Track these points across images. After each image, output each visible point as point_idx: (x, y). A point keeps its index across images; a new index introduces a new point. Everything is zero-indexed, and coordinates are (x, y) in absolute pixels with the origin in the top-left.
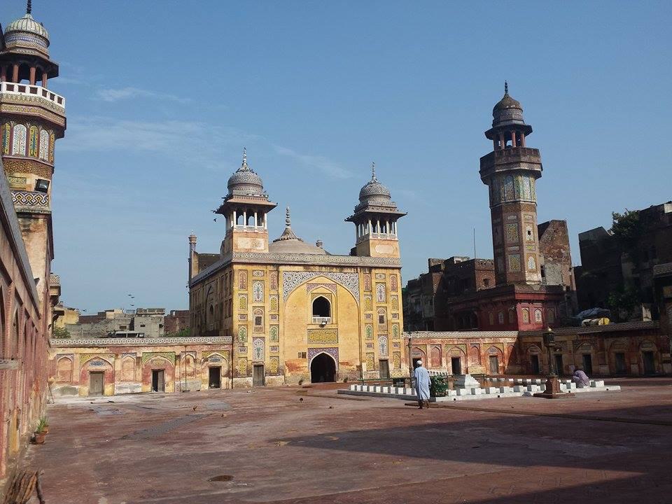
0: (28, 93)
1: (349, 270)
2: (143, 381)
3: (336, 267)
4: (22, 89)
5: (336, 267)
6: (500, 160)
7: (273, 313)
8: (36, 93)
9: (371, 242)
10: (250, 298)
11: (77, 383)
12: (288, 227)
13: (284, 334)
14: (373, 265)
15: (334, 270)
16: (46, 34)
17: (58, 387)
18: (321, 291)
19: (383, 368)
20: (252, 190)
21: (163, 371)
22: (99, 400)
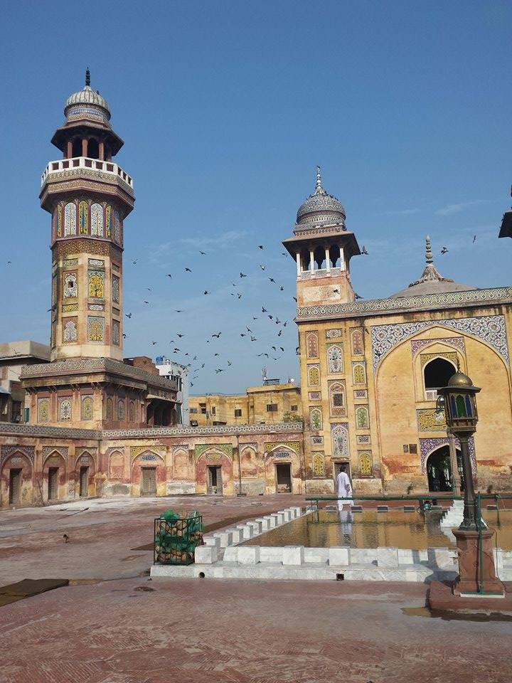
0: (71, 167)
1: (485, 313)
2: (197, 480)
3: (461, 309)
4: (66, 165)
5: (461, 309)
8: (78, 165)
10: (324, 368)
11: (129, 482)
13: (377, 418)
15: (458, 315)
16: (100, 100)
17: (110, 484)
18: (439, 350)
20: (322, 219)
21: (220, 467)
22: (149, 500)
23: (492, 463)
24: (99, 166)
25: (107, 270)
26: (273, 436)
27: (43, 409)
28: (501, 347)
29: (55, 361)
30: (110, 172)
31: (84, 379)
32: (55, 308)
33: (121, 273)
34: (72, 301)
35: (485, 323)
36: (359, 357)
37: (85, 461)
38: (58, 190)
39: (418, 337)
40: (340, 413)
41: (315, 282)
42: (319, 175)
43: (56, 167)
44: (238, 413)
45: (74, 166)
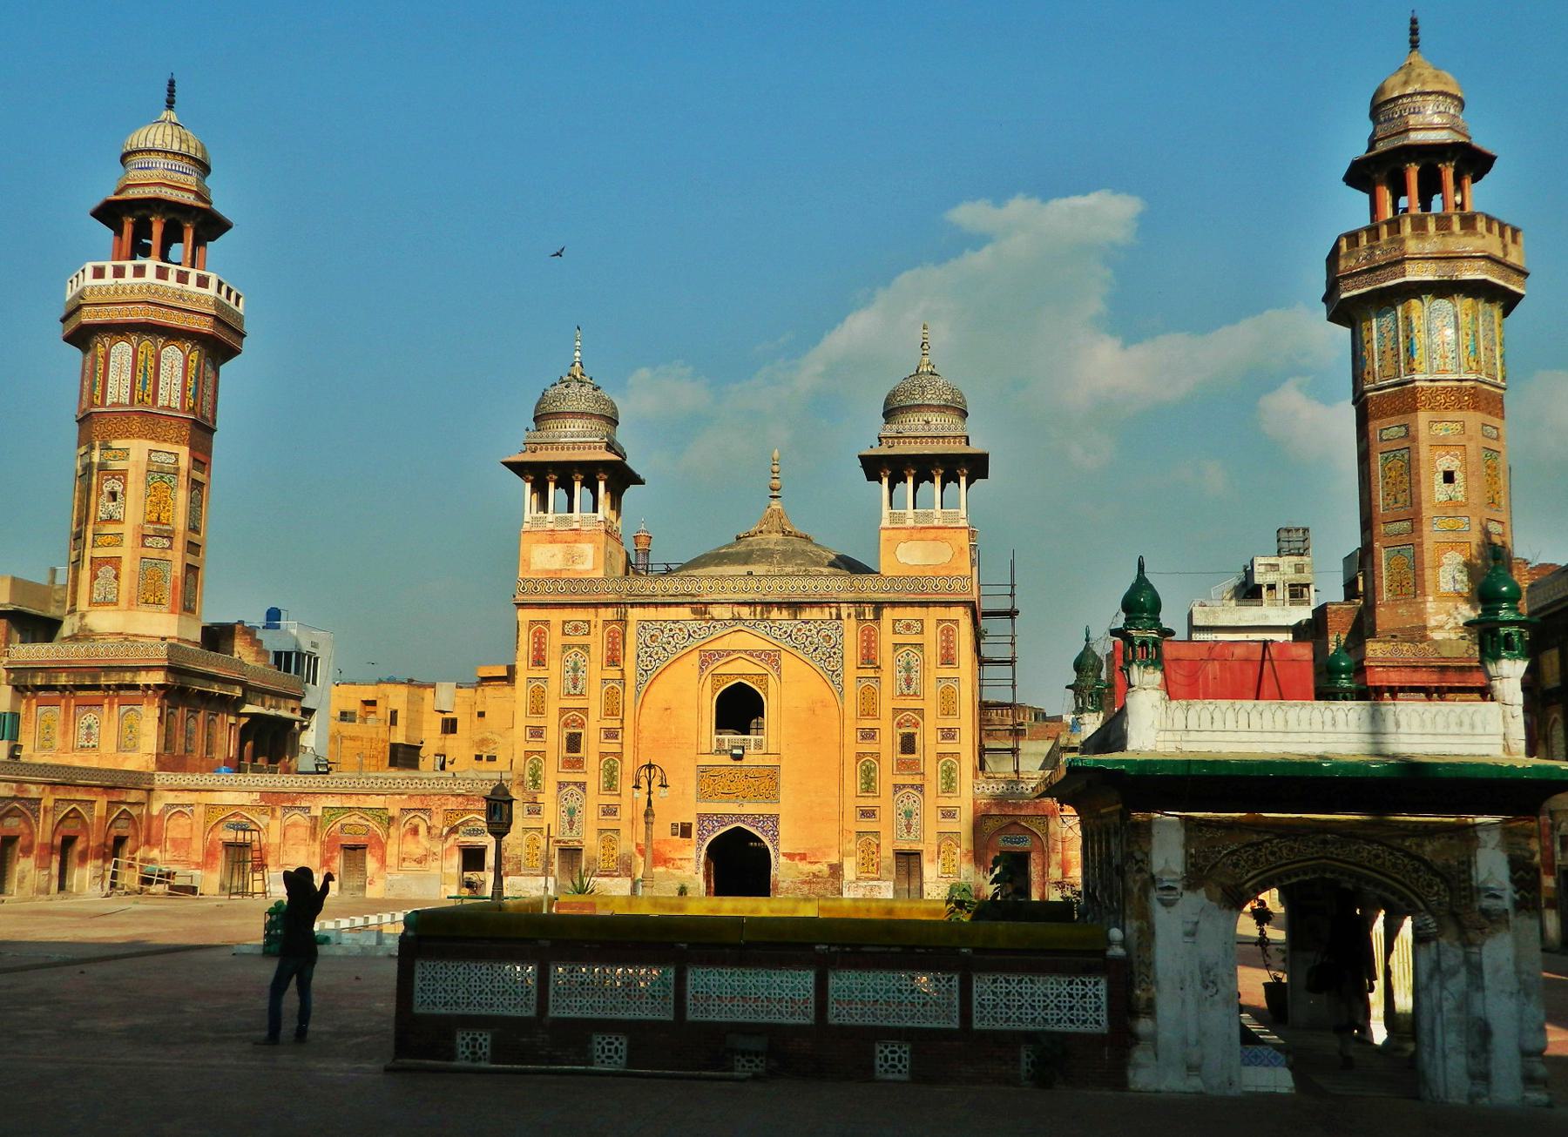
0: (129, 278)
3: (780, 605)
4: (119, 272)
5: (780, 605)
6: (1353, 263)
7: (609, 724)
9: (883, 533)
10: (553, 689)
11: (198, 866)
12: (775, 504)
14: (893, 597)
15: (775, 614)
18: (740, 670)
19: (909, 874)
20: (573, 429)
21: (364, 847)
23: (803, 857)
24: (183, 278)
26: (460, 799)
28: (834, 671)
29: (74, 638)
30: (202, 290)
31: (128, 678)
32: (78, 536)
33: (209, 476)
34: (111, 529)
35: (814, 632)
36: (614, 673)
37: (121, 829)
38: (98, 320)
39: (713, 643)
40: (577, 764)
41: (552, 537)
42: (578, 343)
43: (99, 272)
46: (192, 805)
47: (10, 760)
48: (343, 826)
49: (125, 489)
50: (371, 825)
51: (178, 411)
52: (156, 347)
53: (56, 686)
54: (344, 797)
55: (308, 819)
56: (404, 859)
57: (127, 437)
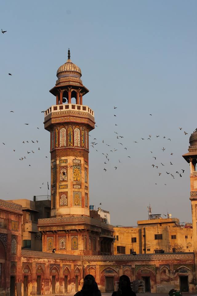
4: (61, 108)
8: (68, 108)
24: (79, 108)
25: (82, 165)
26: (178, 261)
27: (49, 243)
29: (55, 216)
30: (84, 111)
31: (74, 227)
32: (54, 186)
33: (88, 166)
34: (63, 183)
38: (58, 122)
43: (55, 108)
44: (134, 240)
45: (66, 109)
46: (95, 265)
47: (53, 253)
48: (142, 271)
49: (67, 171)
50: (151, 270)
51: (80, 147)
52: (73, 129)
53: (52, 231)
54: (141, 262)
55: (131, 269)
56: (162, 281)
57: (66, 156)
